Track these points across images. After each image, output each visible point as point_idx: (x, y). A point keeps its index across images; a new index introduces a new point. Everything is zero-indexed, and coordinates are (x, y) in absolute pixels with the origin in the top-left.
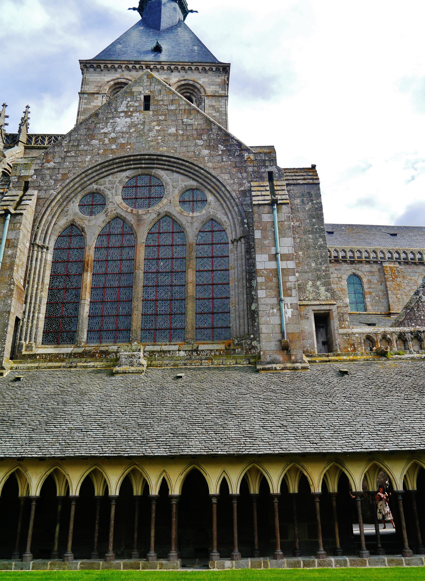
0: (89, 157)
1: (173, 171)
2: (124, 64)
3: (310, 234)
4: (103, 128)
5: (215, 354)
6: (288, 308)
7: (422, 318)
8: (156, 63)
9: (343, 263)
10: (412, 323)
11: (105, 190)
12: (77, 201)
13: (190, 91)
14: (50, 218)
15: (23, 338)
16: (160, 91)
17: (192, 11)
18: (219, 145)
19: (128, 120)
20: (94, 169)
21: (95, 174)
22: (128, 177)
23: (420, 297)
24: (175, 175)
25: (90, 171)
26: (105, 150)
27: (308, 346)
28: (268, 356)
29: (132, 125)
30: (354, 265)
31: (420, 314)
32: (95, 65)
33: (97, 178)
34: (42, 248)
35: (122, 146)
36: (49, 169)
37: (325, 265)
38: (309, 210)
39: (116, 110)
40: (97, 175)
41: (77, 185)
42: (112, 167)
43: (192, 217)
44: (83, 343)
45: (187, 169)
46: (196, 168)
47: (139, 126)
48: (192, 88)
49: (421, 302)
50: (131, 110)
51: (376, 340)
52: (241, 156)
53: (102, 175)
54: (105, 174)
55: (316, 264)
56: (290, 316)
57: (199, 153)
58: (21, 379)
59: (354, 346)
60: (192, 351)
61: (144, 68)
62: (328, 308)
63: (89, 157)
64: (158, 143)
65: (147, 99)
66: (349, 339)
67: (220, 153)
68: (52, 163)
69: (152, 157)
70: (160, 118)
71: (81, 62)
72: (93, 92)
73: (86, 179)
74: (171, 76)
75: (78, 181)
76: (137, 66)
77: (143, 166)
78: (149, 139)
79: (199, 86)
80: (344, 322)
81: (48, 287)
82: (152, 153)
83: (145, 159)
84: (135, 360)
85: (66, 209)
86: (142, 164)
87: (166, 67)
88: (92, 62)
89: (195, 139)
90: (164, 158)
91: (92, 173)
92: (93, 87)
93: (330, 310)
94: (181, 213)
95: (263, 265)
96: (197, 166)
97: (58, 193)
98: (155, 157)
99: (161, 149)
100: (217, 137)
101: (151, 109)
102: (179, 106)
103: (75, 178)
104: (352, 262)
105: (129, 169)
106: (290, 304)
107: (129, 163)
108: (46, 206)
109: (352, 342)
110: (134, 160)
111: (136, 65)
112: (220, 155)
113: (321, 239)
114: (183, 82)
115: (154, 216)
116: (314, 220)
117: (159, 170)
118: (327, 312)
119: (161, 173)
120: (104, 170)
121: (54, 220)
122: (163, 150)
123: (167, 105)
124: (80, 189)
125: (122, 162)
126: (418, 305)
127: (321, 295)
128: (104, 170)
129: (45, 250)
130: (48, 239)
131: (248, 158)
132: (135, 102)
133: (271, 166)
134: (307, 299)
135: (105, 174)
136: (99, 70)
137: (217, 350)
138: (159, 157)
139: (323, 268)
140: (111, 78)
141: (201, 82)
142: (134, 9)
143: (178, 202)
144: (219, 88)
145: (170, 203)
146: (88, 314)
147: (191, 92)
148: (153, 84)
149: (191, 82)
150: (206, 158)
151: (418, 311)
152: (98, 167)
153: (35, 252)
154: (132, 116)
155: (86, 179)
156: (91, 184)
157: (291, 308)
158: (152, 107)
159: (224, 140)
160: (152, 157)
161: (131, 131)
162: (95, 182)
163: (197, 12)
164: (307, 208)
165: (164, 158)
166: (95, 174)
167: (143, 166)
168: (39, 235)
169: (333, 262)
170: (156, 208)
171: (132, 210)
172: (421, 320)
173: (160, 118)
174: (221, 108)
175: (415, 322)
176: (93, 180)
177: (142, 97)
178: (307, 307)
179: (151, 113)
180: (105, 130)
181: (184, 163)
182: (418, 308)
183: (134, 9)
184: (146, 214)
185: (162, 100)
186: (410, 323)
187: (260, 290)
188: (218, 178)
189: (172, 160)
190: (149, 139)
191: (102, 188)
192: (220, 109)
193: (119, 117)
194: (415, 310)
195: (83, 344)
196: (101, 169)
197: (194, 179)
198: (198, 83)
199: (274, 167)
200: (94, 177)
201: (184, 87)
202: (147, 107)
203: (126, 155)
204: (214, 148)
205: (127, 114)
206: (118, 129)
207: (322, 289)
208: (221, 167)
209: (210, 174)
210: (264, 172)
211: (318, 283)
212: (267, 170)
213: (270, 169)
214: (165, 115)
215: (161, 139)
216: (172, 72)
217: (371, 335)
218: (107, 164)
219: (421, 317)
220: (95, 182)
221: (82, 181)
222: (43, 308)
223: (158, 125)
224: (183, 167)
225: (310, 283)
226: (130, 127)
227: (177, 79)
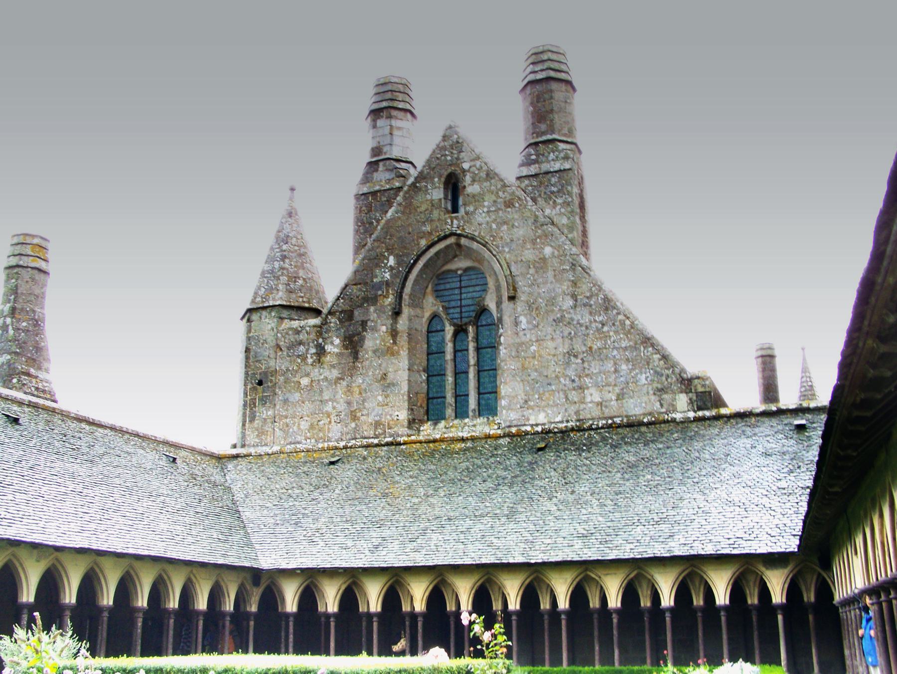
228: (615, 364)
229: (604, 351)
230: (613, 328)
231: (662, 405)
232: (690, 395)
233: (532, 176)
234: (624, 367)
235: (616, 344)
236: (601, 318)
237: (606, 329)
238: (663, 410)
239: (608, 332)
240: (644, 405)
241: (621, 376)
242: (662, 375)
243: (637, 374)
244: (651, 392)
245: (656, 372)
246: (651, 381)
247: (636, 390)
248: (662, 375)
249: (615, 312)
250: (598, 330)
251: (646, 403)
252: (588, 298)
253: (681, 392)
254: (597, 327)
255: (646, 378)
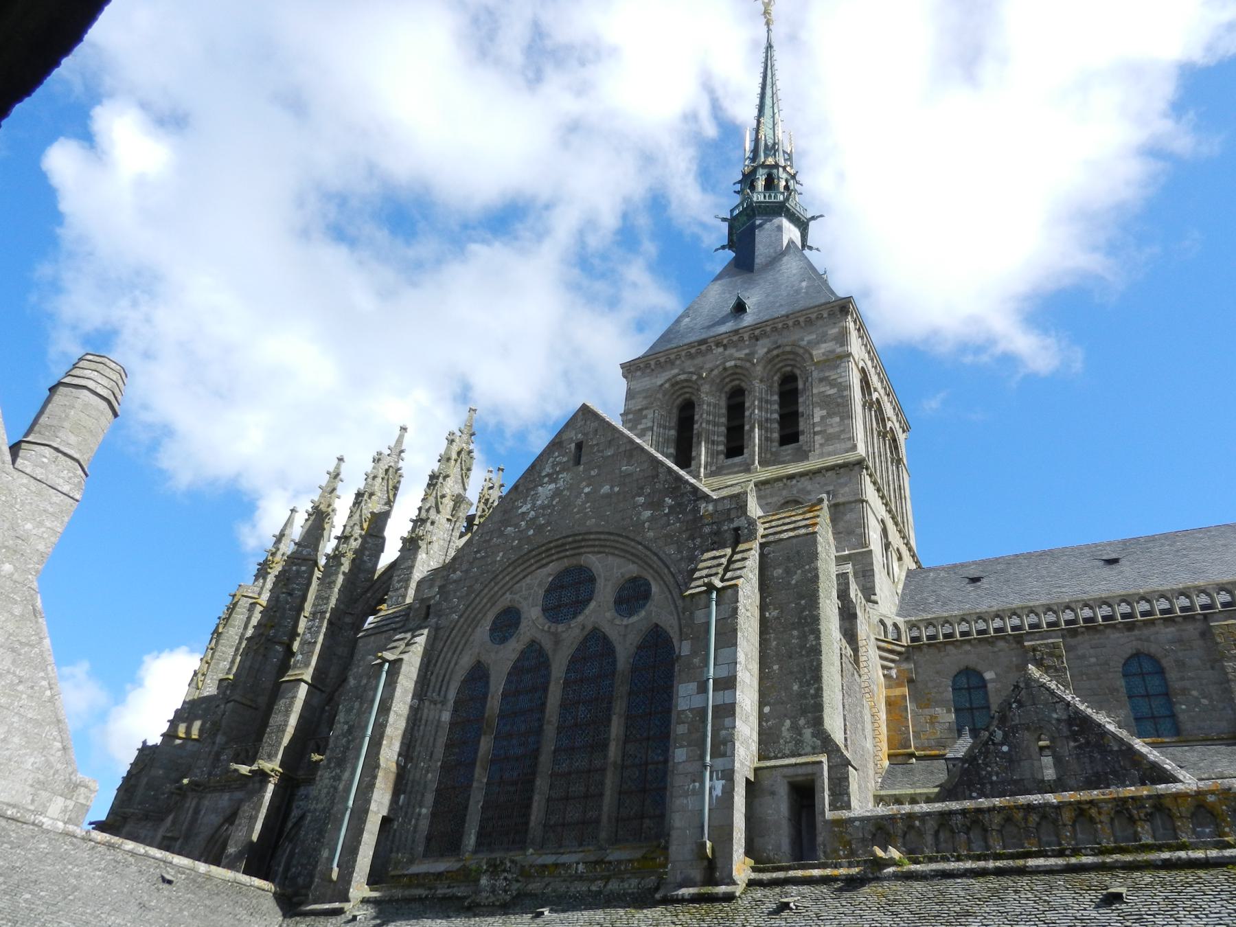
0: (501, 554)
1: (607, 554)
2: (683, 350)
3: (795, 629)
4: (522, 506)
5: (626, 869)
6: (718, 779)
7: (994, 778)
8: (731, 334)
9: (1108, 631)
10: (971, 791)
11: (521, 600)
12: (487, 625)
13: (789, 362)
14: (449, 655)
15: (395, 849)
16: (596, 430)
17: (813, 218)
18: (667, 499)
19: (552, 486)
20: (505, 572)
21: (507, 578)
22: (550, 575)
23: (991, 734)
24: (610, 558)
25: (501, 577)
26: (520, 540)
27: (770, 848)
28: (679, 872)
29: (557, 493)
30: (1136, 632)
31: (988, 772)
32: (642, 365)
33: (510, 584)
34: (435, 704)
35: (540, 529)
36: (455, 581)
37: (816, 686)
38: (796, 584)
39: (539, 476)
40: (512, 579)
41: (485, 600)
42: (529, 563)
43: (626, 626)
44: (467, 854)
45: (623, 547)
46: (633, 543)
47: (565, 493)
48: (791, 356)
49: (994, 744)
50: (558, 469)
51: (892, 832)
52: (696, 510)
53: (517, 579)
54: (521, 576)
55: (801, 686)
56: (720, 794)
57: (638, 518)
58: (358, 918)
59: (851, 847)
60: (596, 863)
61: (713, 347)
62: (809, 769)
63: (501, 554)
64: (586, 514)
65: (579, 446)
66: (841, 832)
67: (667, 511)
68: (458, 573)
69: (577, 538)
70: (593, 473)
71: (623, 366)
72: (640, 407)
73: (496, 589)
74: (757, 348)
75: (486, 595)
76: (703, 347)
77: (568, 553)
78: (575, 510)
79: (801, 351)
80: (841, 797)
81: (439, 764)
82: (577, 532)
83: (570, 543)
84: (497, 884)
85: (471, 639)
86: (567, 550)
87: (746, 337)
88: (636, 362)
89: (633, 497)
90: (592, 537)
91: (504, 577)
92: (641, 399)
93: (814, 774)
94: (612, 621)
95: (688, 702)
96: (633, 540)
97: (460, 617)
98: (581, 537)
99: (588, 523)
100: (664, 486)
101: (582, 462)
102: (618, 448)
103: (482, 590)
104: (1131, 627)
105: (552, 561)
106: (722, 771)
107: (550, 553)
108: (445, 638)
109: (848, 837)
110: (556, 547)
111: (700, 347)
112: (666, 515)
113: (812, 637)
114: (775, 352)
115: (577, 631)
116: (803, 602)
117: (590, 555)
118: (809, 778)
119: (593, 558)
120: (518, 570)
121: (455, 656)
122: (591, 522)
123: (602, 451)
124: (489, 605)
125: (540, 554)
126: (988, 751)
127: (805, 744)
128: (518, 570)
129: (439, 706)
130: (444, 689)
131: (706, 511)
132: (563, 456)
133: (738, 517)
134: (779, 755)
135: (521, 576)
136: (648, 371)
137: (630, 861)
138: (587, 537)
139: (812, 691)
140: (667, 378)
141: (804, 343)
142: (723, 247)
143: (611, 604)
144: (836, 344)
145: (600, 606)
146: (481, 804)
147: (792, 363)
148: (588, 422)
149: (788, 349)
150: (646, 525)
151: (987, 765)
152: (510, 569)
153: (426, 711)
154: (557, 478)
155: (496, 589)
156: (504, 594)
157: (722, 779)
158: (583, 459)
159: (674, 488)
160: (577, 538)
161: (554, 503)
162: (509, 589)
163: (821, 216)
164: (793, 582)
165: (592, 537)
166: (507, 578)
167: (568, 553)
168: (432, 684)
169: (1083, 633)
170: (580, 618)
171: (550, 627)
172: (992, 783)
173: (593, 473)
174: (841, 377)
175: (979, 789)
176: (506, 588)
177: (573, 446)
178: (774, 772)
179: (581, 468)
180: (524, 509)
181: (616, 538)
182: (986, 757)
183: (723, 247)
184: (567, 629)
185: (597, 444)
186: (967, 793)
187: (679, 747)
188: (661, 554)
189: (602, 537)
190: (575, 510)
191: (517, 597)
192: (839, 380)
193: (541, 486)
194: (980, 762)
195: (467, 855)
196: (515, 569)
197: (634, 562)
198: (799, 346)
199: (743, 518)
200: (508, 582)
201: (779, 359)
202: (577, 461)
203: (545, 541)
204: (655, 505)
205: (553, 478)
206: (539, 502)
207: (808, 732)
208: (666, 536)
209: (650, 550)
210: (726, 531)
211: (802, 722)
212: (732, 526)
213: (735, 525)
214: (599, 467)
215: (590, 507)
216: (757, 340)
217: (885, 823)
218: (520, 561)
219: (991, 776)
220: (509, 589)
221: (492, 592)
222: (430, 798)
223: (588, 486)
224: (618, 545)
225: (788, 723)
226: (553, 498)
227: (765, 350)
228: (9, 731)
229: (5, 711)
230: (30, 691)
231: (33, 801)
232: (68, 802)
233: (35, 479)
234: (16, 740)
235: (22, 710)
236: (22, 674)
237: (21, 688)
238: (32, 808)
239: (22, 693)
240: (14, 792)
241: (8, 749)
242: (52, 767)
243: (26, 754)
244: (30, 782)
245: (47, 761)
246: (36, 768)
247: (15, 772)
248: (52, 767)
249: (42, 674)
250: (12, 686)
251: (17, 791)
252: (21, 643)
253: (61, 796)
254: (12, 682)
255: (32, 765)
